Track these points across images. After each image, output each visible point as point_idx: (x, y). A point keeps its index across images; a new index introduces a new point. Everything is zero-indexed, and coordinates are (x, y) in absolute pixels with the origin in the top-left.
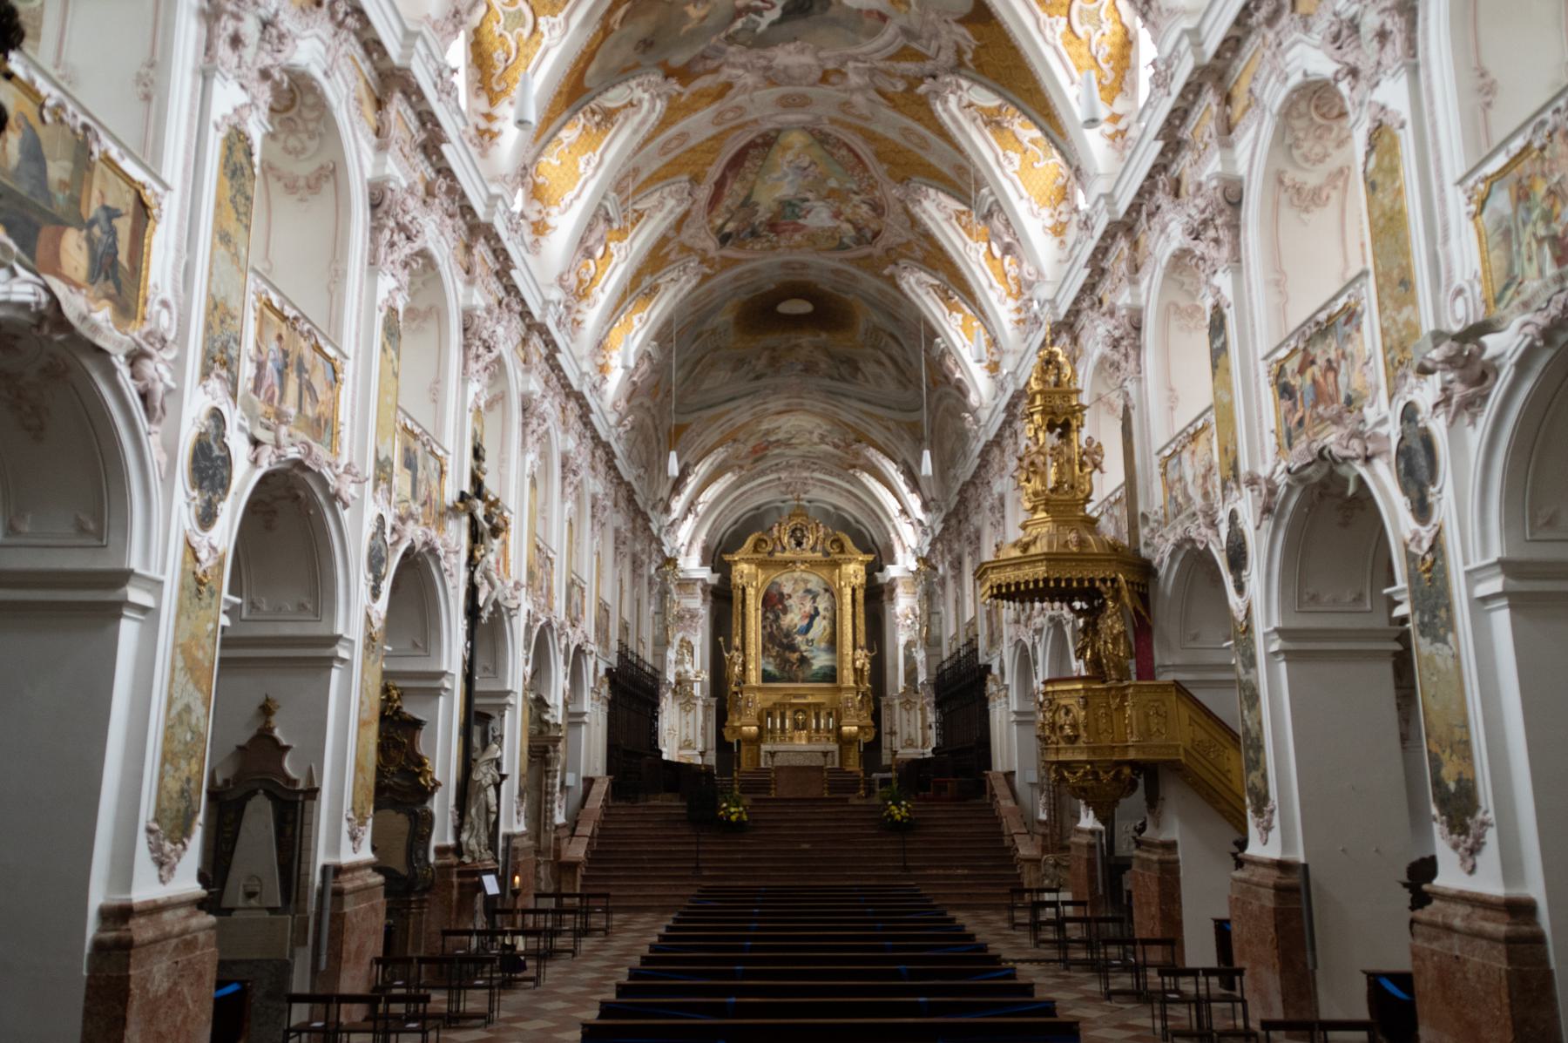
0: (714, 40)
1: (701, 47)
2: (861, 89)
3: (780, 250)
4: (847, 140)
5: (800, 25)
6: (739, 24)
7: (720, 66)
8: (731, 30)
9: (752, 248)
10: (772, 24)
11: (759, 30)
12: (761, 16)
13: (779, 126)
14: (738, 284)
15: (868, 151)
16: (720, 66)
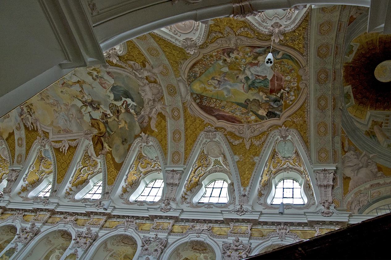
0: (136, 119)
1: (137, 123)
2: (150, 71)
3: (302, 86)
4: (188, 69)
5: (131, 92)
6: (132, 111)
7: (149, 117)
8: (134, 114)
9: (291, 101)
10: (133, 101)
11: (136, 105)
12: (130, 104)
13: (190, 94)
14: (330, 107)
15: (187, 62)
16: (149, 117)
